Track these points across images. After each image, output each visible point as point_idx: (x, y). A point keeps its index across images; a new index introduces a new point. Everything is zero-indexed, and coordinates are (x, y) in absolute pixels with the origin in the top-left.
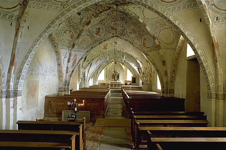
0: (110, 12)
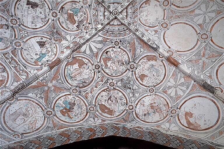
0: (102, 62)
